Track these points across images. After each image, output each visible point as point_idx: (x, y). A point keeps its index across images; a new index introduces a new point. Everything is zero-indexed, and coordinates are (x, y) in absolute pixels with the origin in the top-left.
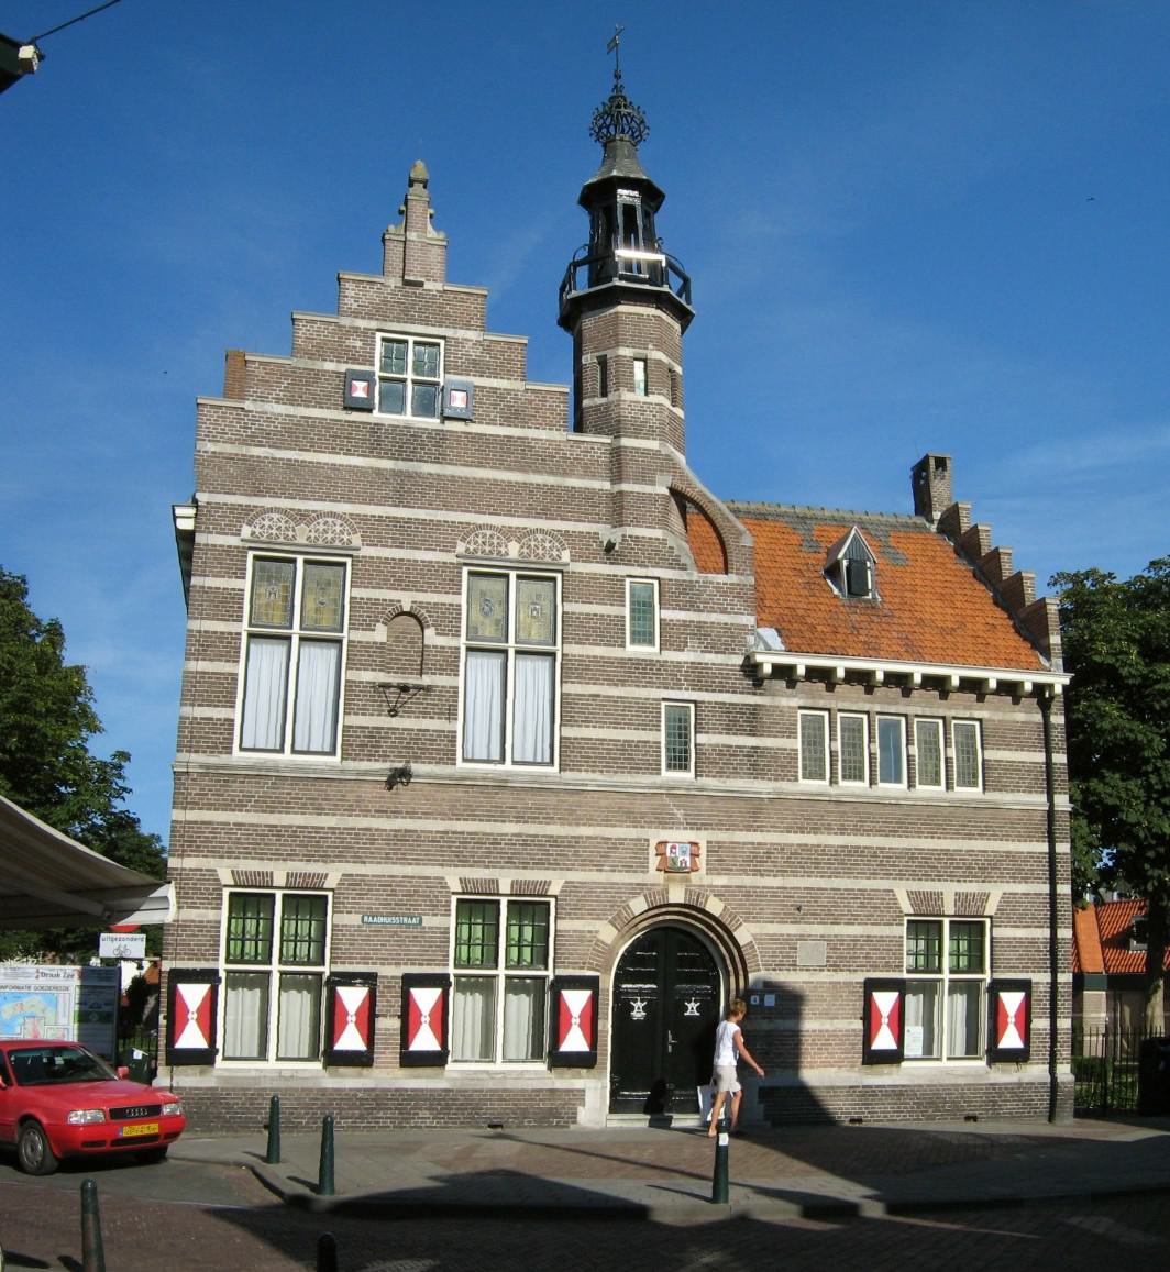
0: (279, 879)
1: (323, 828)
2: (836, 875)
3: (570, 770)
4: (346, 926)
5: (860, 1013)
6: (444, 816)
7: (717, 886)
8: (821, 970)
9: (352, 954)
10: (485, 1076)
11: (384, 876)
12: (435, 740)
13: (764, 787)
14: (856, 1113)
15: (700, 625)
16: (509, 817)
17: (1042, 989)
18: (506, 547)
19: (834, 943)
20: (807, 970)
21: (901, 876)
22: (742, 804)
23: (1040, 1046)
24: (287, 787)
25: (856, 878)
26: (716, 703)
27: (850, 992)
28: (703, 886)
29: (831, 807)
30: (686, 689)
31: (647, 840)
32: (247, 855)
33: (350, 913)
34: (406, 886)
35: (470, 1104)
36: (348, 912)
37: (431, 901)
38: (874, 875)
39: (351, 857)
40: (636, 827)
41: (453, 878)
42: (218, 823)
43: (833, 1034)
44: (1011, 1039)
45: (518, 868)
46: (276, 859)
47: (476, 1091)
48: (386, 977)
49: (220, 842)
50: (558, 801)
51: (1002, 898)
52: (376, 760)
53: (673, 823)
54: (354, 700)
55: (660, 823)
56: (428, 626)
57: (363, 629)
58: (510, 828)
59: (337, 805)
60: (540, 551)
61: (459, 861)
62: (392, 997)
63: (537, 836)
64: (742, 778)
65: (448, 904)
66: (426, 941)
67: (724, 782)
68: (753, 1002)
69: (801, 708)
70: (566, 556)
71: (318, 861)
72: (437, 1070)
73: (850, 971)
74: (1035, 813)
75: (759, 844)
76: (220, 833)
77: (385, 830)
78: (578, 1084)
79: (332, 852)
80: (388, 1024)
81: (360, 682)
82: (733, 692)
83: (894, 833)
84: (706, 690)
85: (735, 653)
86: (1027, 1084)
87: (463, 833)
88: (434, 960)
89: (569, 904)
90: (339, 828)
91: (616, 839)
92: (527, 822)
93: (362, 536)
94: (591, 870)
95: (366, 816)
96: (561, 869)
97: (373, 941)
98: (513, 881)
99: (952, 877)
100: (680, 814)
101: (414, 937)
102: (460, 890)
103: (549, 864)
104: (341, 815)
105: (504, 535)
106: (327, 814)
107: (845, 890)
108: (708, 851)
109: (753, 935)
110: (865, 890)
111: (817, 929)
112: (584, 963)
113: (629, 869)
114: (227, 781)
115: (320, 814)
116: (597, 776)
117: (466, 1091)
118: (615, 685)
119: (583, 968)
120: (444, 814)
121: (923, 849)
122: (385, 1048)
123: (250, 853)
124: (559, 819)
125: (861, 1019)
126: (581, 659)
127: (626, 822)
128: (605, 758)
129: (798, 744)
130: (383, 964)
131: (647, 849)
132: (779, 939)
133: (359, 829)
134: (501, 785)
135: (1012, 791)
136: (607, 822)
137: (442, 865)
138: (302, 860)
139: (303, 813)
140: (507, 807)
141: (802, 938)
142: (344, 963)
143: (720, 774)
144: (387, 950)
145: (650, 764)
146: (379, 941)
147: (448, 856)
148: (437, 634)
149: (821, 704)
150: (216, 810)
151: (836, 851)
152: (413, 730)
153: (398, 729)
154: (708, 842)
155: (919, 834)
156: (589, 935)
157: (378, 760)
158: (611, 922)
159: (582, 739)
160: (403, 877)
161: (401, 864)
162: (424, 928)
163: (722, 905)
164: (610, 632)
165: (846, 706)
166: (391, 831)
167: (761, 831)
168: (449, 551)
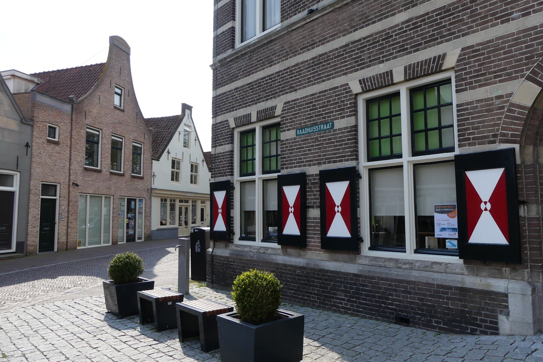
6: (346, 32)
10: (392, 264)
11: (307, 96)
35: (378, 293)
47: (382, 279)
48: (312, 175)
65: (355, 105)
66: (337, 142)
71: (271, 98)
72: (352, 256)
87: (360, 40)
88: (344, 156)
89: (470, 73)
98: (405, 68)
112: (495, 136)
117: (373, 278)
119: (494, 142)
130: (310, 165)
137: (346, 74)
142: (287, 168)
144: (312, 154)
147: (350, 64)
156: (497, 102)
158: (529, 78)
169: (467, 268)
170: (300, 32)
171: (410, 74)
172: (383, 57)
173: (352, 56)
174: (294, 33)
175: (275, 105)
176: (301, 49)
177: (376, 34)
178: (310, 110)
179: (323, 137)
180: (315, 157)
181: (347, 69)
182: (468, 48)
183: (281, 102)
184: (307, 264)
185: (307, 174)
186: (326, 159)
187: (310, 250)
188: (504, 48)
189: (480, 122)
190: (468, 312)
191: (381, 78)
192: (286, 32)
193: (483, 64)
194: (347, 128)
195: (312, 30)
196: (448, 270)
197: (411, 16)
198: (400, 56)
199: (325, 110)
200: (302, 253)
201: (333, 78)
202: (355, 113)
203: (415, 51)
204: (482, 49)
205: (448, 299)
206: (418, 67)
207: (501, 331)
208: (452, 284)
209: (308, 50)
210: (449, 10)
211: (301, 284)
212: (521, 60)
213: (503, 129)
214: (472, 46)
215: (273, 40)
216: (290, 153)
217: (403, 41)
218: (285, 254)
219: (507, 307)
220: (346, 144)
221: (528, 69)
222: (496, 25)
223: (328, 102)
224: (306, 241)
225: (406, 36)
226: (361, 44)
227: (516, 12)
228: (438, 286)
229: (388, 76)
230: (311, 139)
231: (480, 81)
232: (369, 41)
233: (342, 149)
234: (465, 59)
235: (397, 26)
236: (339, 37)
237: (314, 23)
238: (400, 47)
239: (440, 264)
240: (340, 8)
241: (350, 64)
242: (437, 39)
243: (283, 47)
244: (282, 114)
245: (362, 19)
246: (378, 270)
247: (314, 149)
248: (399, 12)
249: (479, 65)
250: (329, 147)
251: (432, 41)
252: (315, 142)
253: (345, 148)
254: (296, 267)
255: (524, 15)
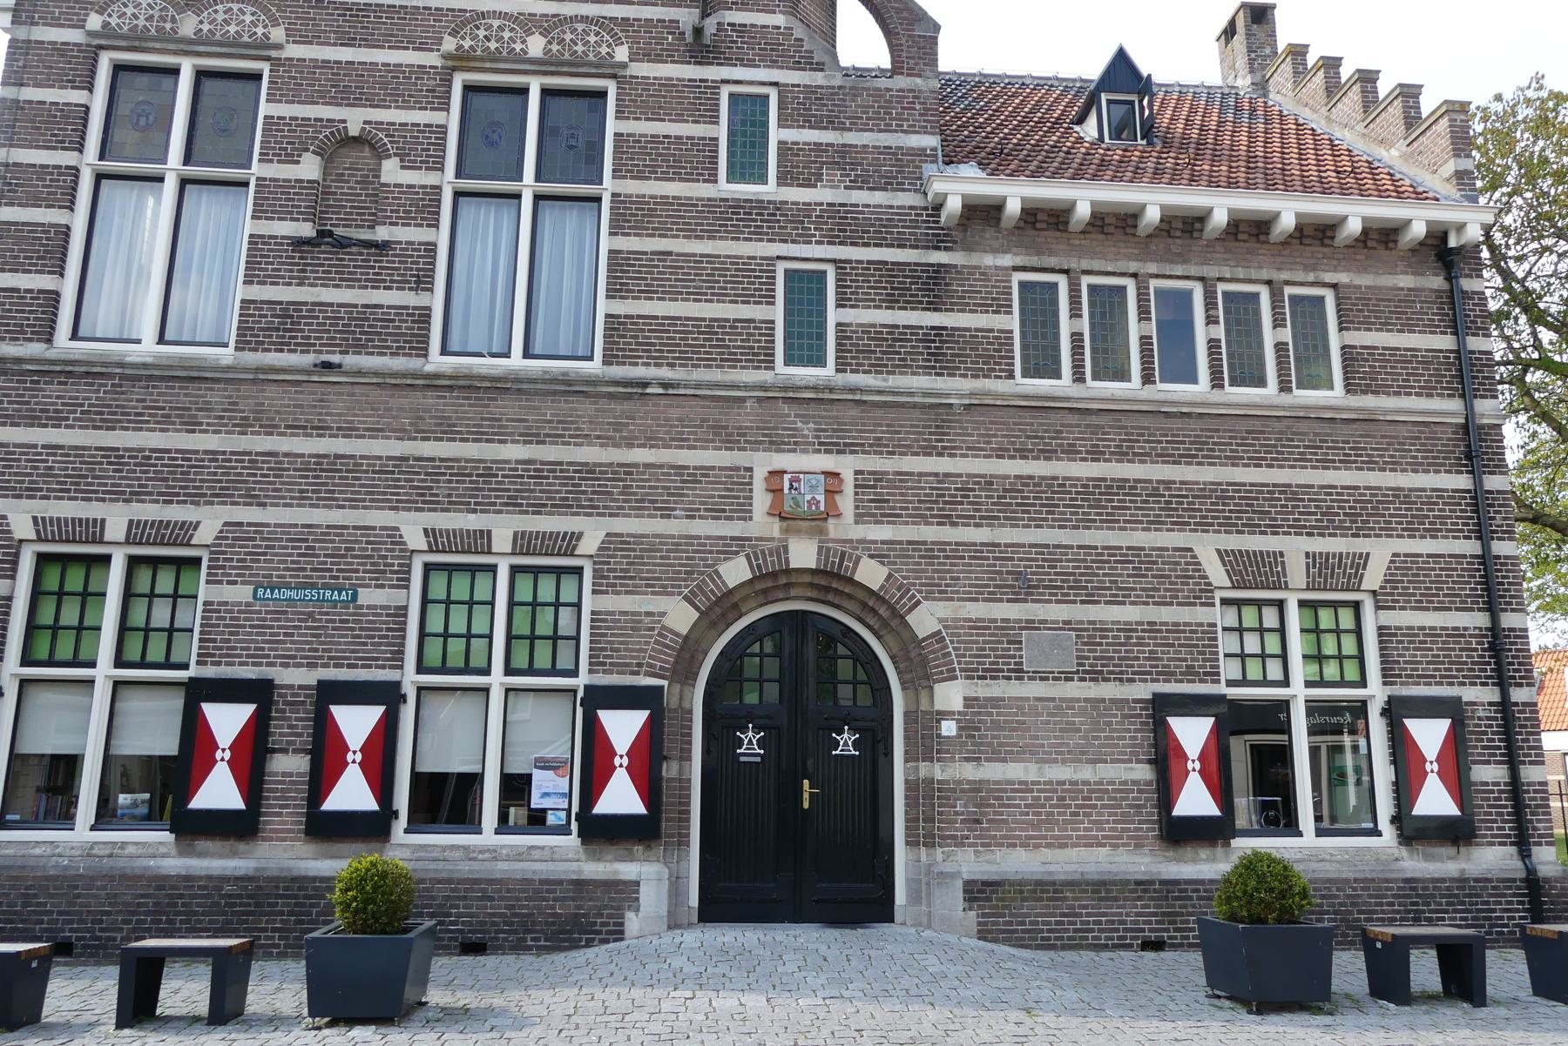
0: (116, 529)
1: (196, 452)
2: (1087, 523)
3: (618, 364)
4: (226, 603)
5: (1146, 752)
6: (403, 434)
7: (875, 542)
8: (1067, 679)
9: (235, 648)
10: (458, 854)
12: (393, 321)
13: (957, 387)
14: (1151, 930)
15: (845, 149)
16: (512, 434)
17: (1481, 714)
18: (524, 42)
19: (1090, 634)
20: (1042, 679)
21: (1203, 526)
22: (916, 414)
23: (1493, 816)
24: (137, 392)
25: (1121, 529)
26: (869, 262)
27: (1124, 716)
28: (851, 541)
29: (1073, 419)
30: (818, 243)
31: (750, 469)
32: (63, 493)
33: (235, 583)
34: (333, 541)
36: (229, 583)
37: (373, 564)
38: (1155, 524)
39: (240, 496)
40: (731, 449)
41: (413, 529)
42: (15, 445)
43: (1098, 789)
44: (1435, 800)
45: (526, 512)
46: (111, 500)
47: (439, 882)
48: (291, 687)
49: (16, 474)
50: (597, 410)
51: (1391, 562)
52: (290, 351)
53: (796, 443)
54: (260, 263)
55: (771, 443)
56: (389, 157)
57: (279, 162)
58: (515, 452)
59: (222, 418)
60: (580, 48)
61: (424, 502)
62: (297, 719)
63: (561, 463)
64: (914, 374)
65: (406, 570)
66: (361, 629)
67: (886, 380)
68: (954, 733)
69: (1016, 269)
70: (622, 53)
71: (185, 502)
73: (1121, 680)
74: (1439, 429)
75: (947, 475)
76: (19, 460)
77: (302, 455)
78: (627, 870)
79: (209, 488)
80: (289, 765)
81: (271, 237)
82: (899, 246)
83: (1189, 458)
84: (852, 244)
85: (904, 190)
86: (1477, 880)
87: (432, 459)
88: (377, 659)
89: (615, 570)
90: (224, 453)
91: (695, 468)
92: (543, 443)
93: (286, 29)
94: (650, 516)
95: (271, 434)
96: (599, 515)
97: (271, 627)
98: (516, 534)
99: (1298, 529)
100: (807, 429)
101: (341, 621)
102: (426, 548)
103: (579, 507)
104: (227, 432)
105: (522, 25)
106: (206, 431)
107: (1104, 548)
108: (856, 486)
109: (940, 620)
110: (1143, 549)
111: (1057, 612)
112: (639, 665)
113: (717, 513)
114: (38, 382)
115: (193, 431)
116: (665, 373)
118: (697, 237)
119: (637, 673)
120: (405, 431)
121: (1244, 485)
122: (281, 807)
123: (68, 491)
124: (598, 437)
125: (1150, 762)
126: (641, 200)
127: (713, 441)
128: (679, 345)
129: (1013, 322)
130: (285, 665)
131: (750, 484)
132: (989, 628)
133: (258, 454)
134: (500, 386)
135: (1398, 394)
136: (682, 442)
137: (396, 509)
138: (157, 502)
139: (162, 430)
140: (508, 420)
141: (1030, 625)
142: (218, 664)
143: (877, 368)
144: (293, 642)
145: (754, 354)
146: (279, 627)
147: (406, 494)
148: (403, 167)
149: (1052, 261)
150: (13, 425)
151: (1084, 486)
152: (356, 306)
153: (331, 305)
154: (857, 472)
155: (1234, 461)
156: (646, 620)
157: (295, 351)
158: (686, 598)
159: (639, 317)
160: (328, 527)
161: (325, 506)
162: (361, 607)
163: (883, 572)
164: (698, 162)
165: (1097, 265)
166: (310, 456)
167: (951, 455)
168: (432, 50)
169: (586, 851)
170: (290, 392)
171: (522, 546)
172: (476, 504)
173: (412, 480)
174: (274, 387)
175: (194, 521)
176: (287, 427)
177: (467, 461)
178: (300, 555)
179: (327, 614)
180: (303, 650)
181: (397, 501)
182: (616, 535)
183: (216, 518)
184: (257, 869)
185: (277, 682)
186: (330, 658)
187: (264, 839)
188: (661, 550)
189: (621, 643)
190: (584, 915)
191: (469, 538)
192: (251, 376)
193: (633, 563)
194: (389, 607)
195: (321, 401)
196: (556, 856)
197: (534, 457)
198: (508, 512)
199: (339, 563)
200: (242, 846)
201: (365, 508)
202: (405, 584)
203: (534, 513)
204: (634, 543)
205: (555, 900)
206: (537, 539)
207: (627, 934)
208: (563, 877)
209: (306, 435)
210: (593, 472)
211: (233, 914)
212: (679, 572)
213: (651, 657)
214: (621, 535)
215: (206, 378)
216: (231, 633)
217: (516, 490)
218: (182, 853)
219: (637, 899)
220: (381, 637)
221: (686, 587)
222: (654, 516)
223: (347, 549)
224: (258, 822)
225: (521, 484)
226: (433, 467)
227: (680, 509)
228: (542, 882)
229: (482, 537)
230: (293, 613)
231: (627, 585)
232: (452, 467)
233: (373, 644)
234: (609, 549)
235: (507, 462)
236: (388, 438)
237: (330, 389)
238: (509, 498)
239: (542, 848)
240: (395, 385)
241: (406, 494)
242: (571, 506)
243: (236, 404)
244: (214, 545)
245: (440, 424)
246: (432, 866)
247: (300, 635)
248: (513, 442)
249: (628, 564)
250: (341, 636)
251: (563, 507)
252: (306, 621)
253: (380, 644)
254: (225, 879)
255: (688, 517)
